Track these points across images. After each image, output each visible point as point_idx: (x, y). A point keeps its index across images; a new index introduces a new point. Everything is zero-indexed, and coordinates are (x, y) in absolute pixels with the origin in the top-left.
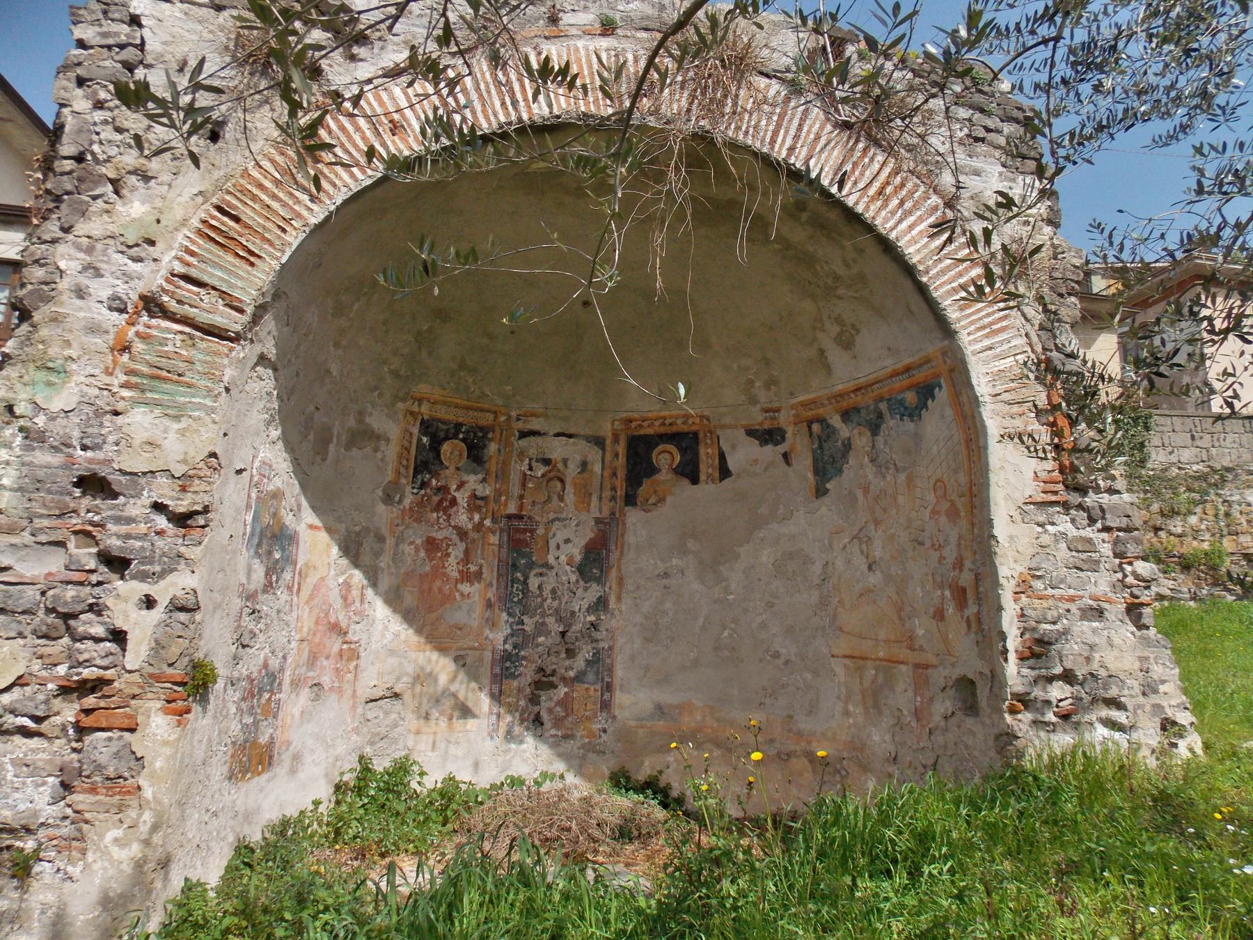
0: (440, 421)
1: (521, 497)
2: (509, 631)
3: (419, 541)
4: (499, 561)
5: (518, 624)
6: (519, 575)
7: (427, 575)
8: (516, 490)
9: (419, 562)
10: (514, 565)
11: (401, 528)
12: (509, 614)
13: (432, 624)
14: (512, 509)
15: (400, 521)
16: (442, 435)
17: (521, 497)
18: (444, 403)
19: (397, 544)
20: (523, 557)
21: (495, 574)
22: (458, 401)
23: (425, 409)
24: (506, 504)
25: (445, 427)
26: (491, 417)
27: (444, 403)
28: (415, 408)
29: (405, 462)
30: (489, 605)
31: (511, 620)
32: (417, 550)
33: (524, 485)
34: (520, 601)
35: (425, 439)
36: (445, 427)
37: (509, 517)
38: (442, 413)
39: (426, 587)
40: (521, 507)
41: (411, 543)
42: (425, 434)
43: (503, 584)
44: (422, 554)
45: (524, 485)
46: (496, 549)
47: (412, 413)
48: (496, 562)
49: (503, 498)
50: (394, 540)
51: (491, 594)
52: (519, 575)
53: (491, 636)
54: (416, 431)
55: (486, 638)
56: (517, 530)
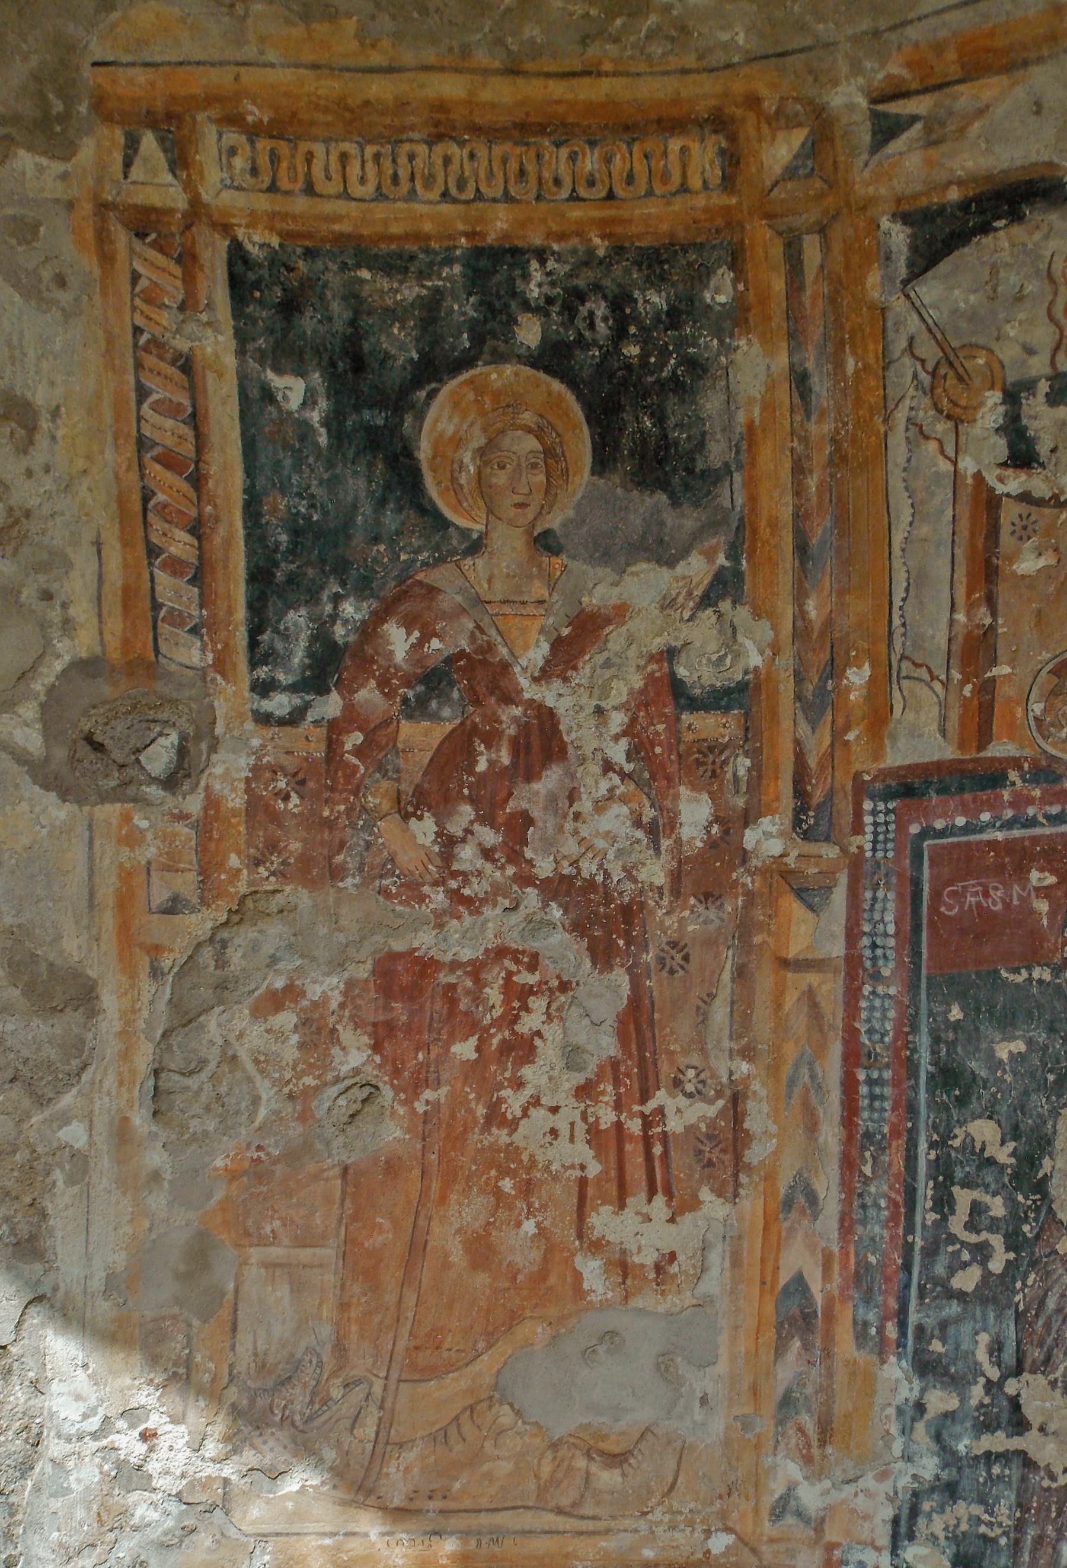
0: (359, 251)
1: (977, 650)
2: (929, 1467)
3: (325, 987)
4: (853, 1056)
5: (985, 1425)
6: (984, 1131)
7: (392, 1167)
8: (935, 619)
9: (332, 1104)
10: (949, 1076)
11: (199, 923)
12: (926, 1367)
13: (441, 1437)
14: (922, 736)
15: (187, 883)
16: (400, 345)
17: (977, 650)
18: (354, 120)
19: (185, 1018)
20: (1007, 1023)
21: (831, 1135)
22: (450, 87)
23: (221, 174)
24: (878, 718)
25: (410, 292)
26: (703, 156)
27: (354, 120)
28: (157, 185)
29: (180, 544)
30: (798, 1317)
31: (940, 1400)
32: (318, 1034)
33: (986, 572)
34: (993, 1293)
35: (292, 390)
36: (410, 292)
37: (909, 787)
38: (352, 194)
39: (384, 1236)
40: (981, 718)
41: (276, 1001)
42: (288, 354)
43: (881, 1191)
44: (354, 1054)
45: (986, 572)
46: (830, 989)
47: (145, 223)
48: (832, 1068)
49: (857, 677)
50: (154, 999)
51: (804, 1257)
52: (984, 1131)
53: (811, 1497)
54: (216, 343)
55: (782, 1507)
56: (966, 862)
